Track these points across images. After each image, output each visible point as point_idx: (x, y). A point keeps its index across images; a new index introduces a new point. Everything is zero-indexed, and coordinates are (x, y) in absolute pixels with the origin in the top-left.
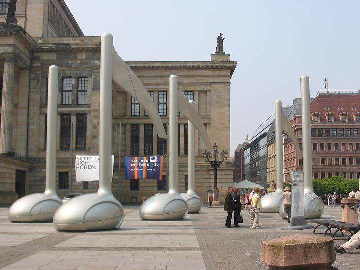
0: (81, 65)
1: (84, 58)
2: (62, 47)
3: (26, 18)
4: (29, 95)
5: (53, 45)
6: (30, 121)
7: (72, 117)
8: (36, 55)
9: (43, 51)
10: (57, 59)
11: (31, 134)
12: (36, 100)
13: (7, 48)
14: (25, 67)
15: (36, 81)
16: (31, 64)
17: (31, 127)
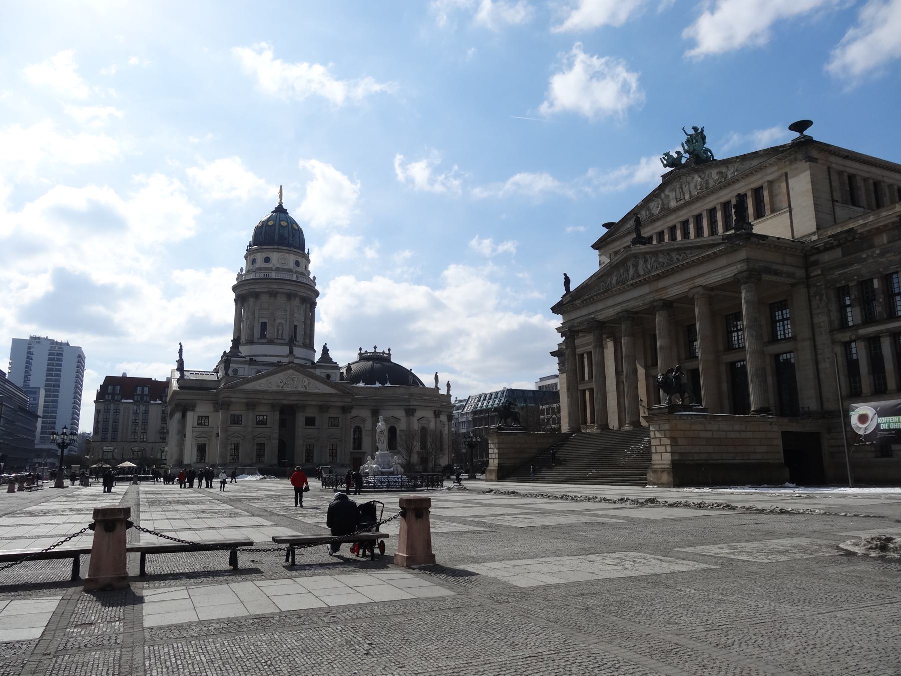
0: (882, 254)
1: (885, 241)
2: (844, 235)
3: (790, 211)
4: (812, 318)
5: (829, 237)
6: (820, 357)
7: (882, 339)
8: (813, 258)
9: (818, 251)
10: (843, 256)
11: (822, 376)
12: (822, 324)
13: (739, 266)
14: (794, 281)
15: (818, 297)
16: (808, 277)
17: (822, 366)
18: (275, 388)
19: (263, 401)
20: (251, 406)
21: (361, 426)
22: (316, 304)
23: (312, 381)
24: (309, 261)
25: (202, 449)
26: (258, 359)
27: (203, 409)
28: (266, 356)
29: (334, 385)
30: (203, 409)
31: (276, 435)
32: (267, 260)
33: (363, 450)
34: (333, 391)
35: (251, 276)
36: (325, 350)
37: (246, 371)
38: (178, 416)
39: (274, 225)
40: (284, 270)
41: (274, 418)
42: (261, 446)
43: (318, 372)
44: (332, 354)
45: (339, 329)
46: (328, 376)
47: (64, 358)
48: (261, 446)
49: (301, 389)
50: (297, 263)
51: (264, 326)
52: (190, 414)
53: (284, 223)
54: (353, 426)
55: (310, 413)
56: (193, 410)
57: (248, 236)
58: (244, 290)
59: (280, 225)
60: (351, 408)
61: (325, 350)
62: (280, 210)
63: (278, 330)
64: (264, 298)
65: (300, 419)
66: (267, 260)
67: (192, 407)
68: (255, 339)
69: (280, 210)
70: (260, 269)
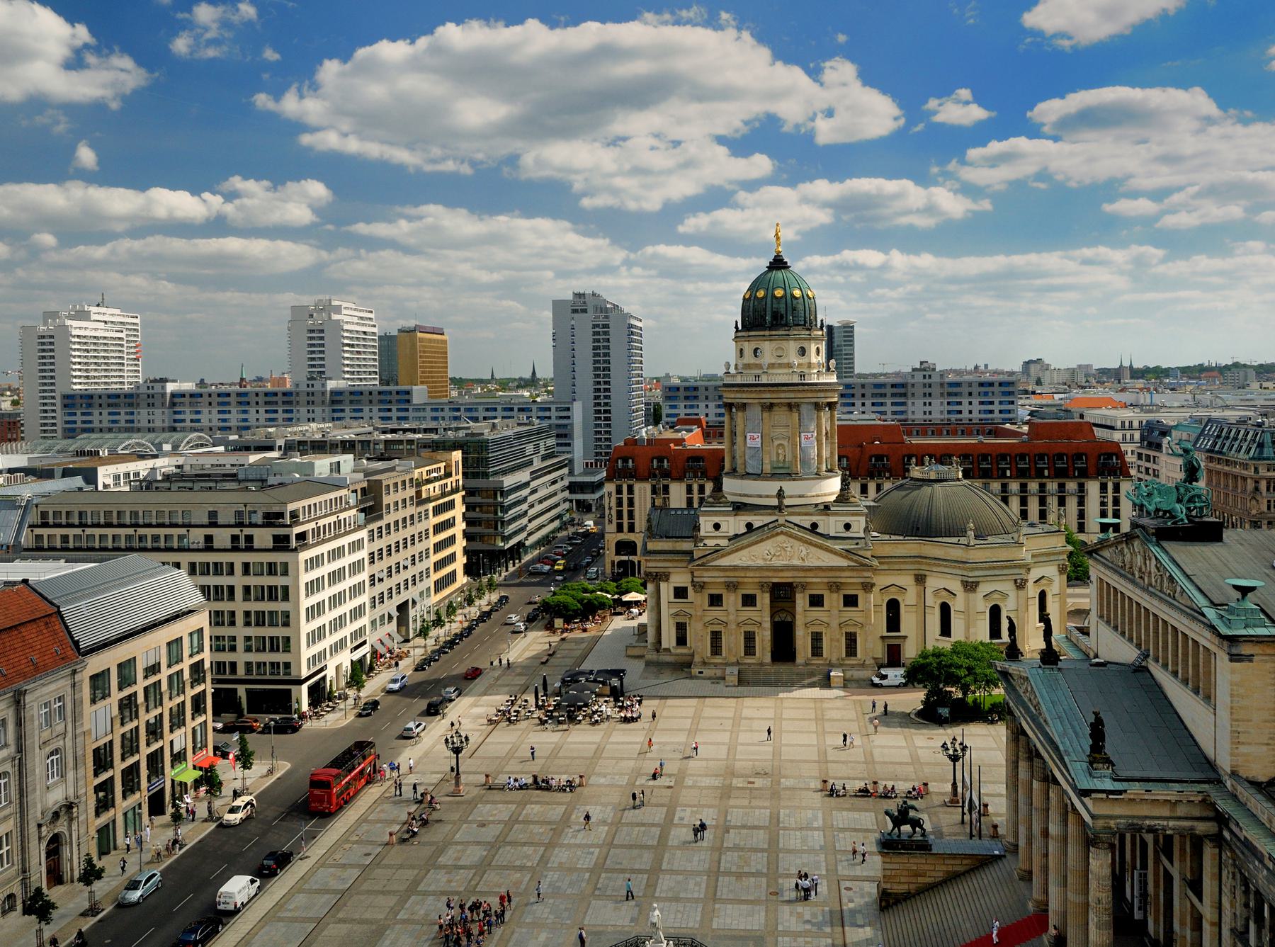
18: (760, 562)
20: (732, 586)
21: (900, 599)
23: (813, 549)
25: (681, 628)
28: (760, 496)
34: (844, 563)
39: (765, 297)
41: (764, 600)
42: (750, 638)
47: (611, 330)
48: (750, 638)
49: (796, 562)
52: (663, 585)
53: (779, 293)
54: (887, 599)
56: (667, 580)
59: (773, 296)
64: (755, 412)
65: (801, 601)
70: (747, 366)
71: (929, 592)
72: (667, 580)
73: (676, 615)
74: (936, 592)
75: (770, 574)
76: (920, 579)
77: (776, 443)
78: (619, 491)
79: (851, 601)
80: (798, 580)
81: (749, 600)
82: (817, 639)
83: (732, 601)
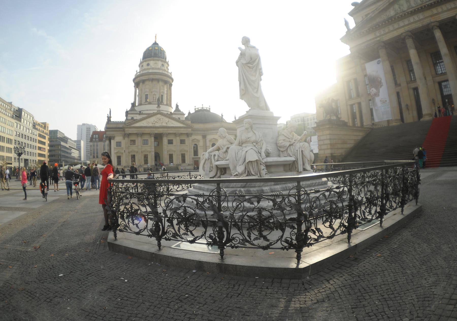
18: (151, 125)
19: (145, 132)
21: (197, 144)
22: (172, 85)
23: (170, 120)
24: (168, 65)
25: (119, 158)
26: (144, 112)
27: (119, 138)
28: (147, 110)
29: (182, 122)
30: (119, 138)
31: (153, 150)
32: (148, 65)
33: (199, 157)
35: (141, 73)
36: (177, 106)
37: (137, 117)
38: (107, 142)
39: (152, 49)
40: (156, 69)
41: (151, 140)
43: (174, 116)
44: (180, 108)
45: (185, 98)
46: (179, 118)
49: (164, 124)
50: (163, 65)
51: (147, 96)
52: (112, 141)
53: (157, 48)
55: (170, 138)
56: (114, 139)
57: (140, 56)
58: (137, 80)
60: (191, 134)
61: (177, 106)
62: (155, 44)
63: (153, 97)
65: (165, 140)
66: (148, 65)
67: (113, 138)
68: (143, 103)
69: (155, 44)
70: (145, 69)
71: (207, 141)
72: (114, 139)
73: (117, 153)
74: (210, 141)
75: (154, 130)
76: (204, 137)
77: (153, 93)
78: (94, 146)
79: (182, 142)
80: (165, 132)
81: (145, 142)
82: (171, 156)
83: (139, 141)
